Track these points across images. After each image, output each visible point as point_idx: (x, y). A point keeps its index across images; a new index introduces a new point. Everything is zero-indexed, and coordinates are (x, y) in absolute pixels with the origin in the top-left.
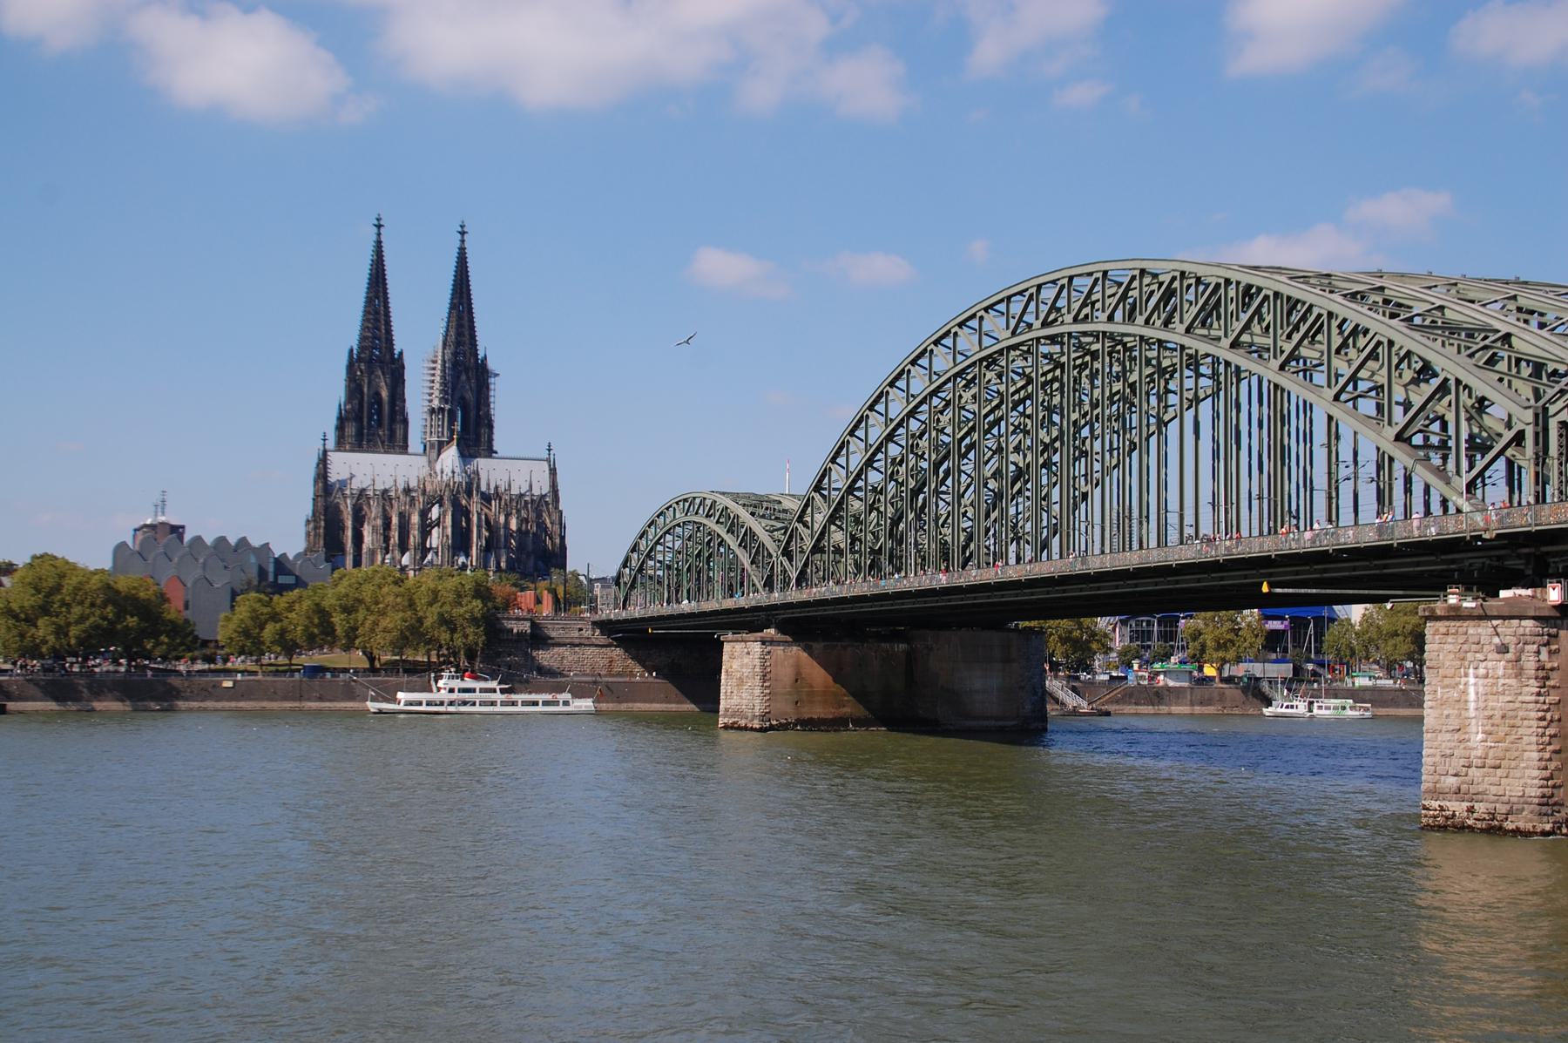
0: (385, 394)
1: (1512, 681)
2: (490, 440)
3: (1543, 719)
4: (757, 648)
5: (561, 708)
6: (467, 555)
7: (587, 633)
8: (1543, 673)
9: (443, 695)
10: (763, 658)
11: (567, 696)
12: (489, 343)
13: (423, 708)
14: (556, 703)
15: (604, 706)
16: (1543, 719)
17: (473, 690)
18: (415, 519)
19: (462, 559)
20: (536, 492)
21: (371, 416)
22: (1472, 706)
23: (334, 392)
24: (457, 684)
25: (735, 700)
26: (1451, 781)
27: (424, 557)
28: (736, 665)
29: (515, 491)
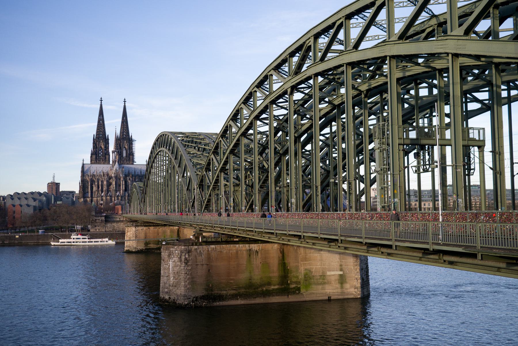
0: (103, 147)
1: (179, 263)
2: (133, 159)
3: (186, 273)
4: (134, 229)
5: (105, 243)
6: (120, 193)
7: (122, 219)
8: (187, 262)
9: (72, 240)
10: (135, 231)
11: (107, 239)
12: (133, 131)
13: (66, 244)
14: (104, 242)
15: (118, 241)
16: (186, 273)
17: (80, 239)
18: (105, 183)
19: (118, 193)
20: (142, 174)
21: (99, 153)
22: (171, 270)
23: (90, 147)
24: (75, 237)
25: (129, 244)
26: (166, 290)
27: (107, 194)
28: (129, 234)
29: (136, 174)
